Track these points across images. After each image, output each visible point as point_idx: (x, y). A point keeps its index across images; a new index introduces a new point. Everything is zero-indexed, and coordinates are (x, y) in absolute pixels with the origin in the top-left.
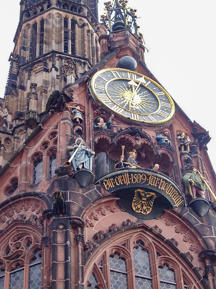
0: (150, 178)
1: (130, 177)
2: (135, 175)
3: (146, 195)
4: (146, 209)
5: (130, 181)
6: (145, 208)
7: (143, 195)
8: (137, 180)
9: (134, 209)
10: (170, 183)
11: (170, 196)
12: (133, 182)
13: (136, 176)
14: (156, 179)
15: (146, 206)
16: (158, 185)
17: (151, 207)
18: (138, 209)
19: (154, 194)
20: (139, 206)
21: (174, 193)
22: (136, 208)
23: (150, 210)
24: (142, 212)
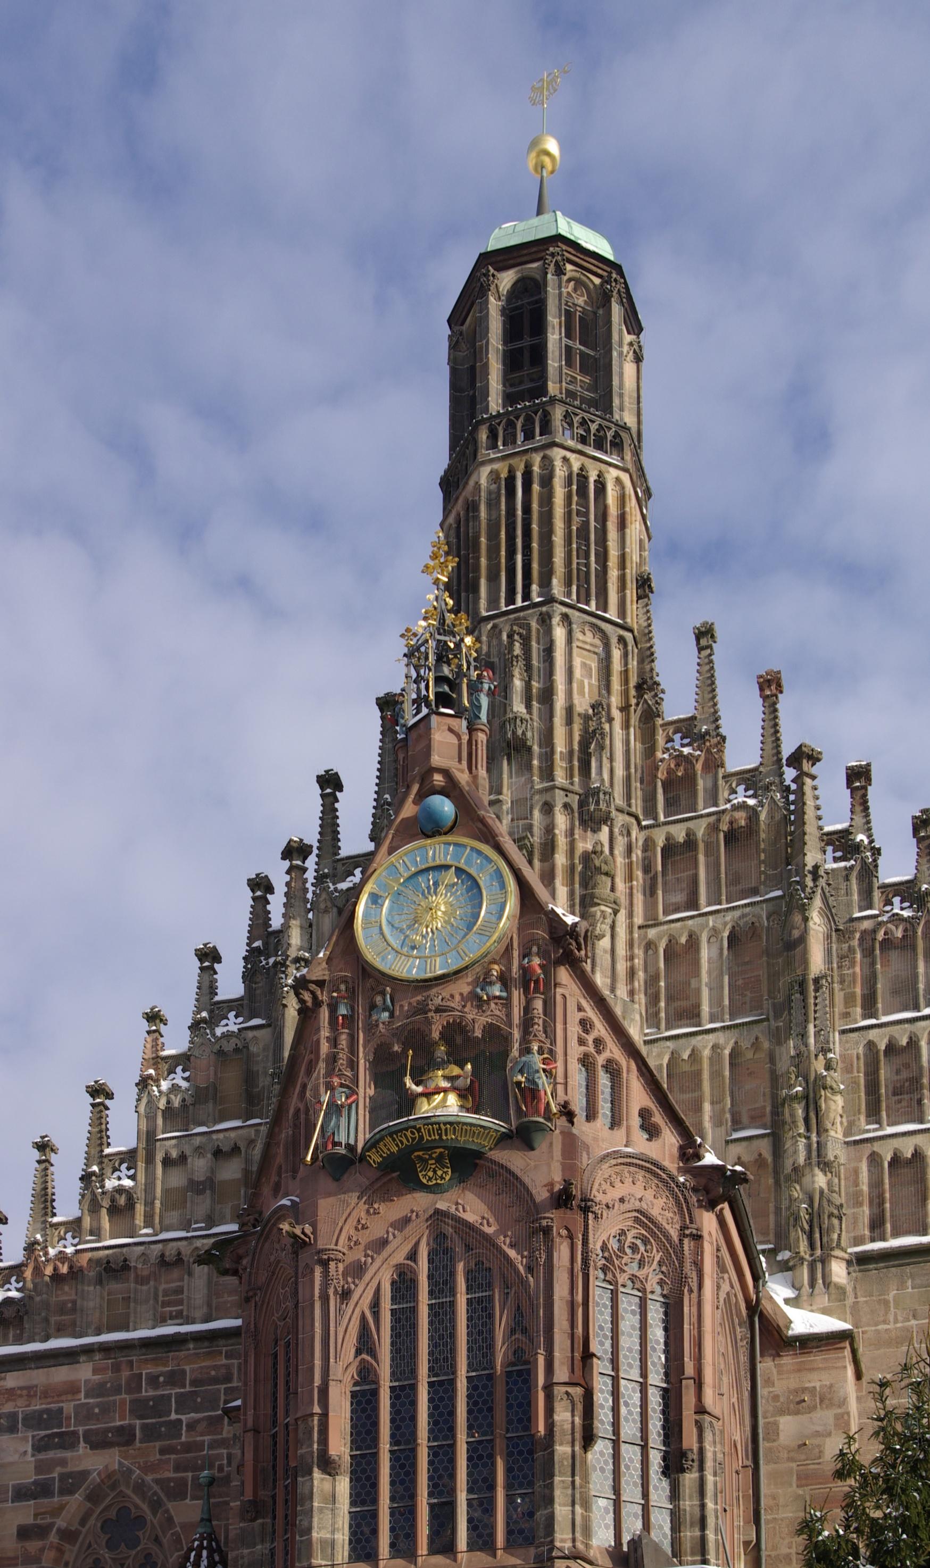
1: (394, 1140)
3: (430, 1155)
5: (397, 1145)
6: (439, 1173)
7: (427, 1157)
8: (405, 1141)
9: (424, 1181)
16: (440, 1135)
18: (430, 1179)
19: (442, 1150)
20: (431, 1174)
24: (439, 1181)
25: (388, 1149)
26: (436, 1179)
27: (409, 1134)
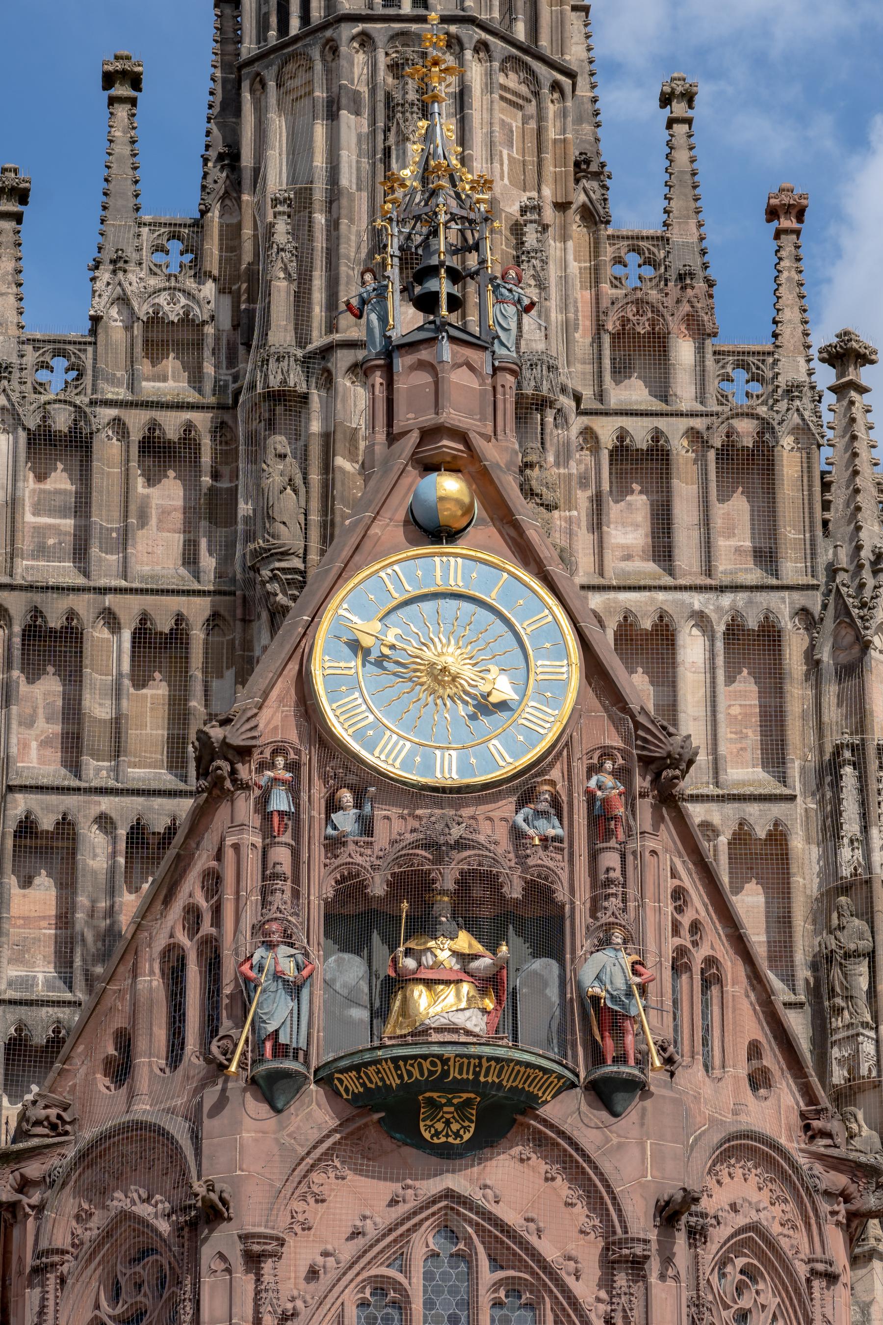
1: (397, 1068)
2: (410, 1062)
4: (458, 1131)
5: (401, 1077)
6: (455, 1127)
7: (444, 1101)
9: (427, 1135)
12: (406, 1078)
13: (412, 1065)
15: (457, 1121)
17: (471, 1121)
18: (437, 1134)
20: (440, 1126)
22: (433, 1131)
23: (472, 1130)
24: (450, 1140)
25: (382, 1079)
26: (447, 1136)
27: (426, 1065)
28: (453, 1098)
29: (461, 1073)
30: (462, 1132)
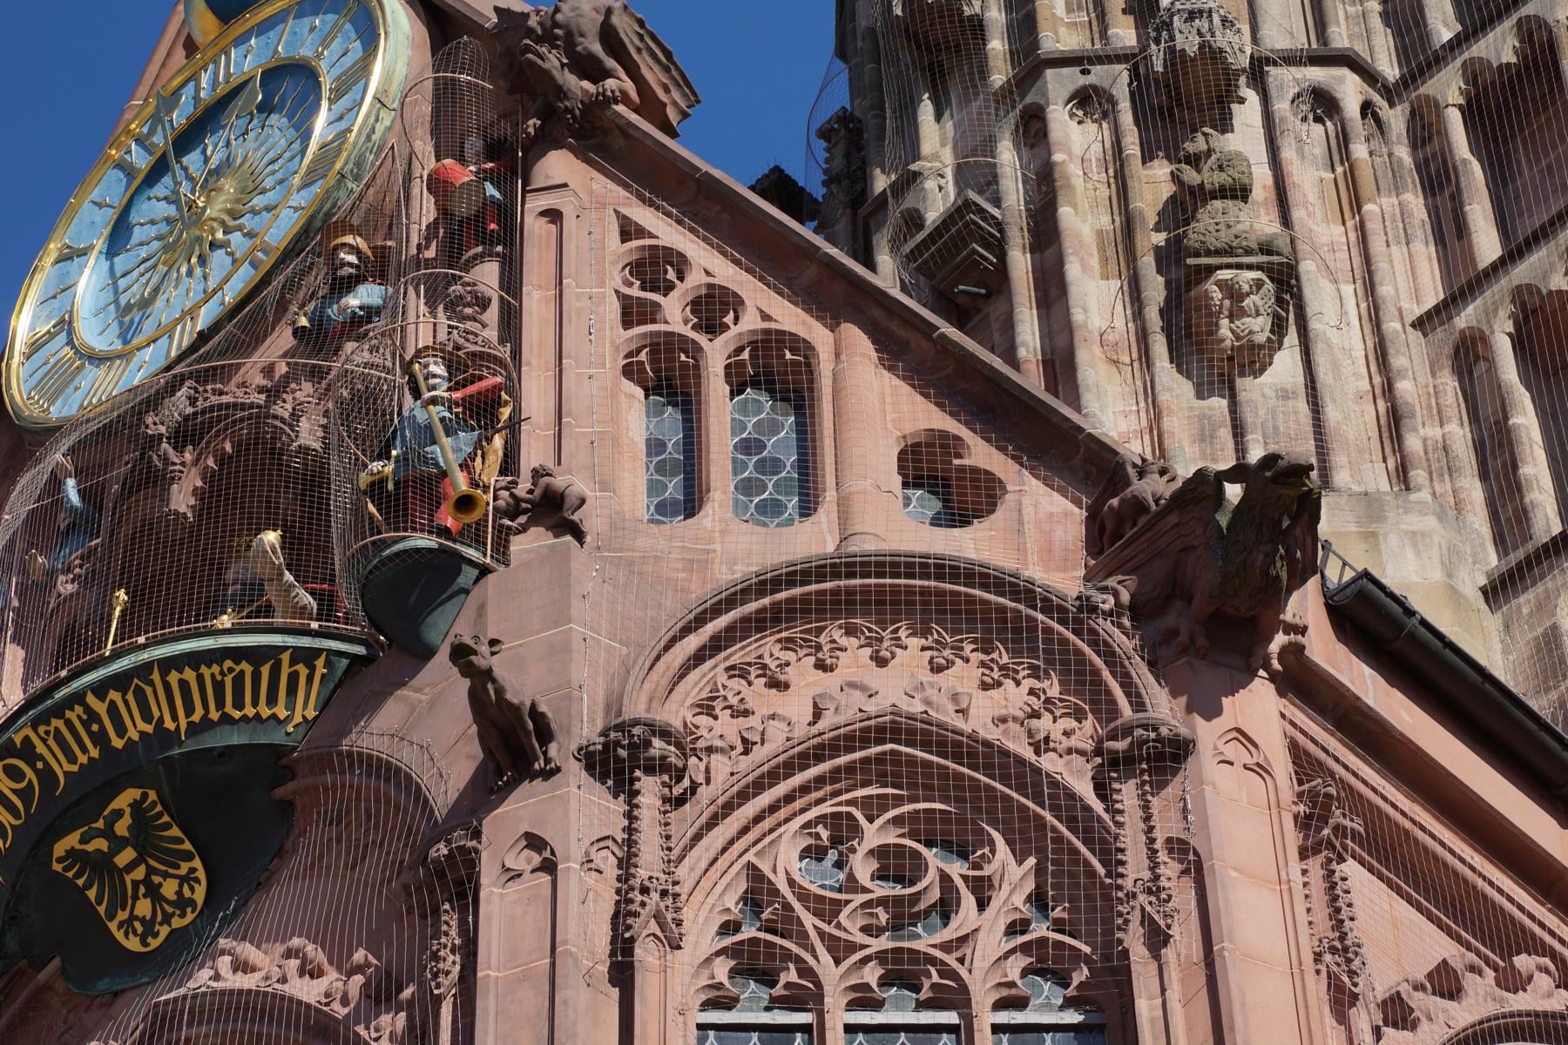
0: (40, 748)
3: (108, 833)
4: (179, 893)
6: (169, 889)
7: (101, 844)
9: (133, 944)
10: (144, 670)
11: (214, 715)
14: (68, 723)
15: (166, 875)
16: (101, 739)
17: (188, 857)
20: (144, 907)
21: (219, 687)
23: (201, 874)
24: (177, 923)
26: (167, 919)
28: (110, 824)
29: (72, 759)
30: (187, 892)
